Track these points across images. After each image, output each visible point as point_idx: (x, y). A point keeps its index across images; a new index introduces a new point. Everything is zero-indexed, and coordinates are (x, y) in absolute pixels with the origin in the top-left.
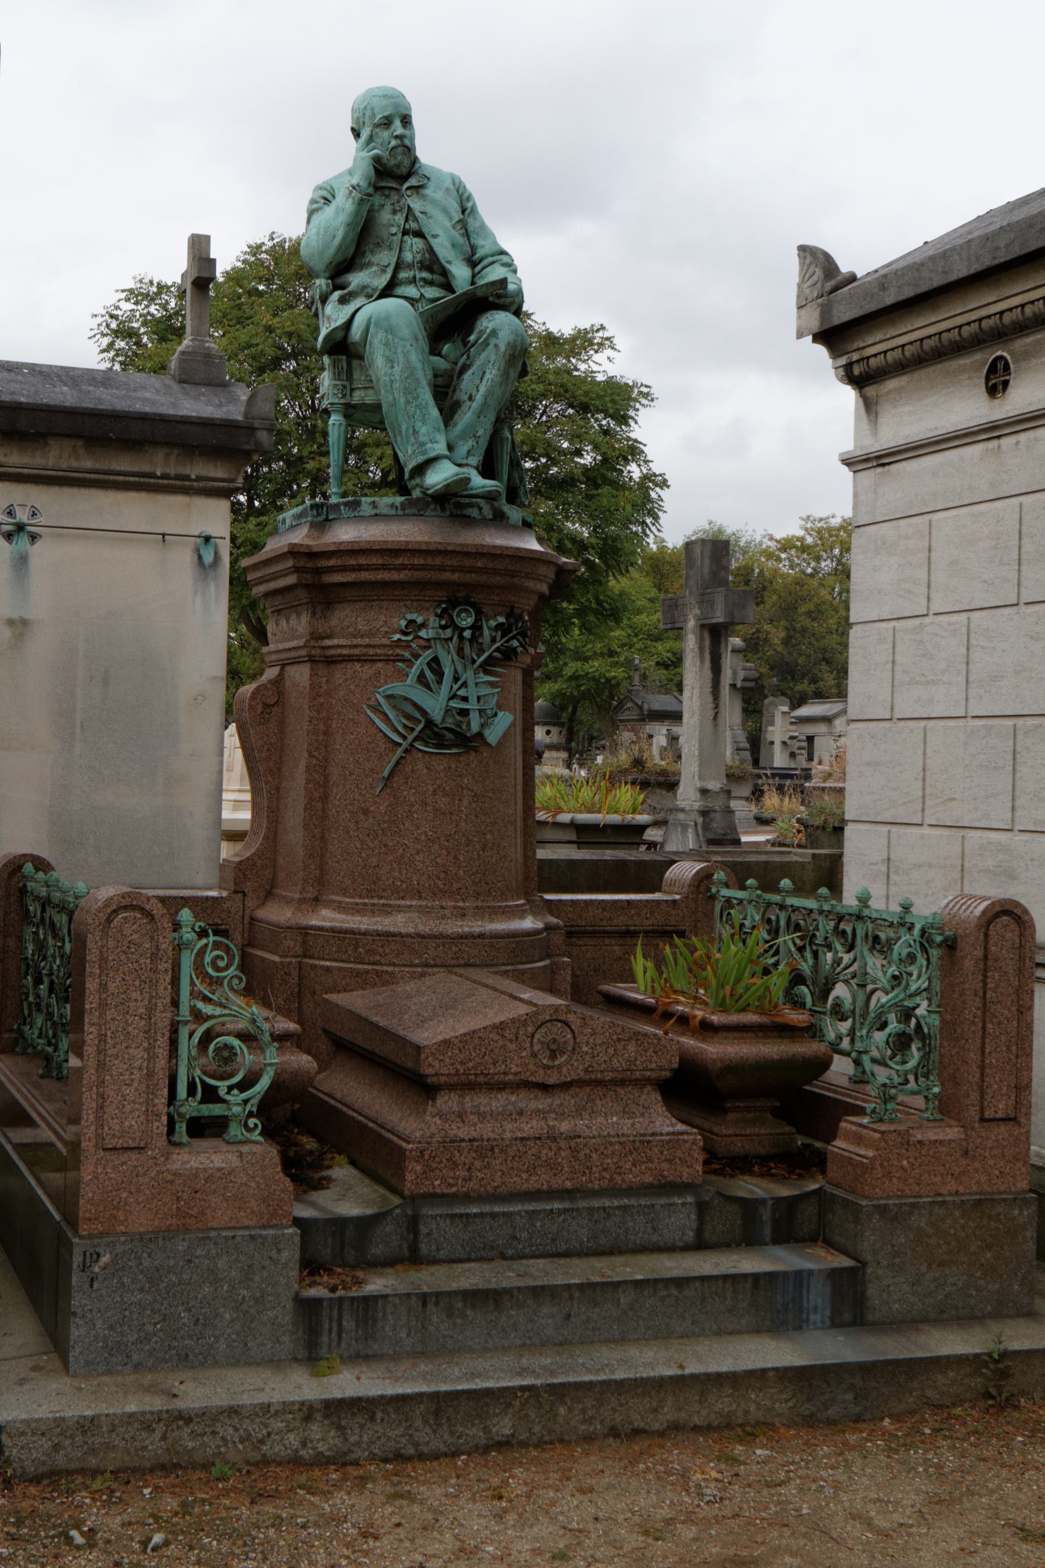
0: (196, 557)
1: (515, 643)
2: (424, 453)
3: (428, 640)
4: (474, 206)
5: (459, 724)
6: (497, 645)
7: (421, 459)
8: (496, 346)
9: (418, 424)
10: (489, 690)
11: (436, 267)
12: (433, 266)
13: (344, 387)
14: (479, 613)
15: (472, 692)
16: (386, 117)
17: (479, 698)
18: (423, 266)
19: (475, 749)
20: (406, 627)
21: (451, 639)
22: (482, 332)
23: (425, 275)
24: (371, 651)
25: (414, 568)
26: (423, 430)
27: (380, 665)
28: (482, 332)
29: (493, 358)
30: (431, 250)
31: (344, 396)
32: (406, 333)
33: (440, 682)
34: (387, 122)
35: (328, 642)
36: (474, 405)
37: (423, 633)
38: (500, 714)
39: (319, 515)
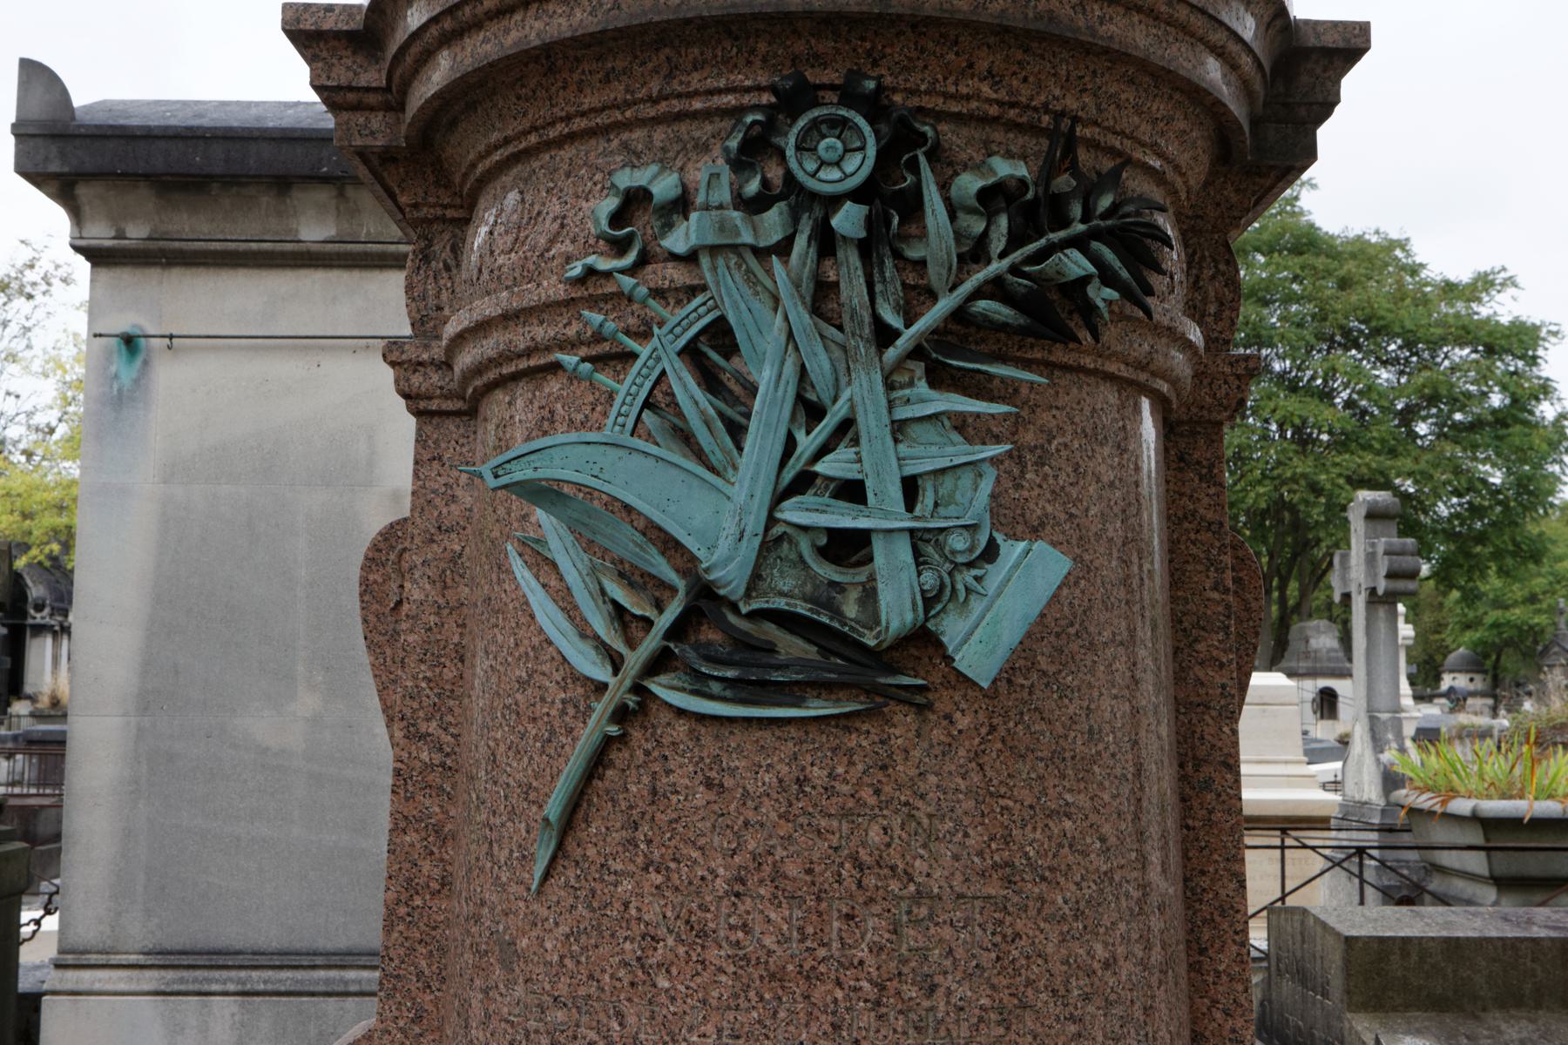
1: (1075, 264)
5: (827, 597)
6: (996, 267)
10: (959, 451)
15: (877, 462)
17: (911, 488)
19: (918, 701)
20: (617, 219)
21: (783, 248)
33: (736, 431)
37: (678, 240)
38: (1012, 551)
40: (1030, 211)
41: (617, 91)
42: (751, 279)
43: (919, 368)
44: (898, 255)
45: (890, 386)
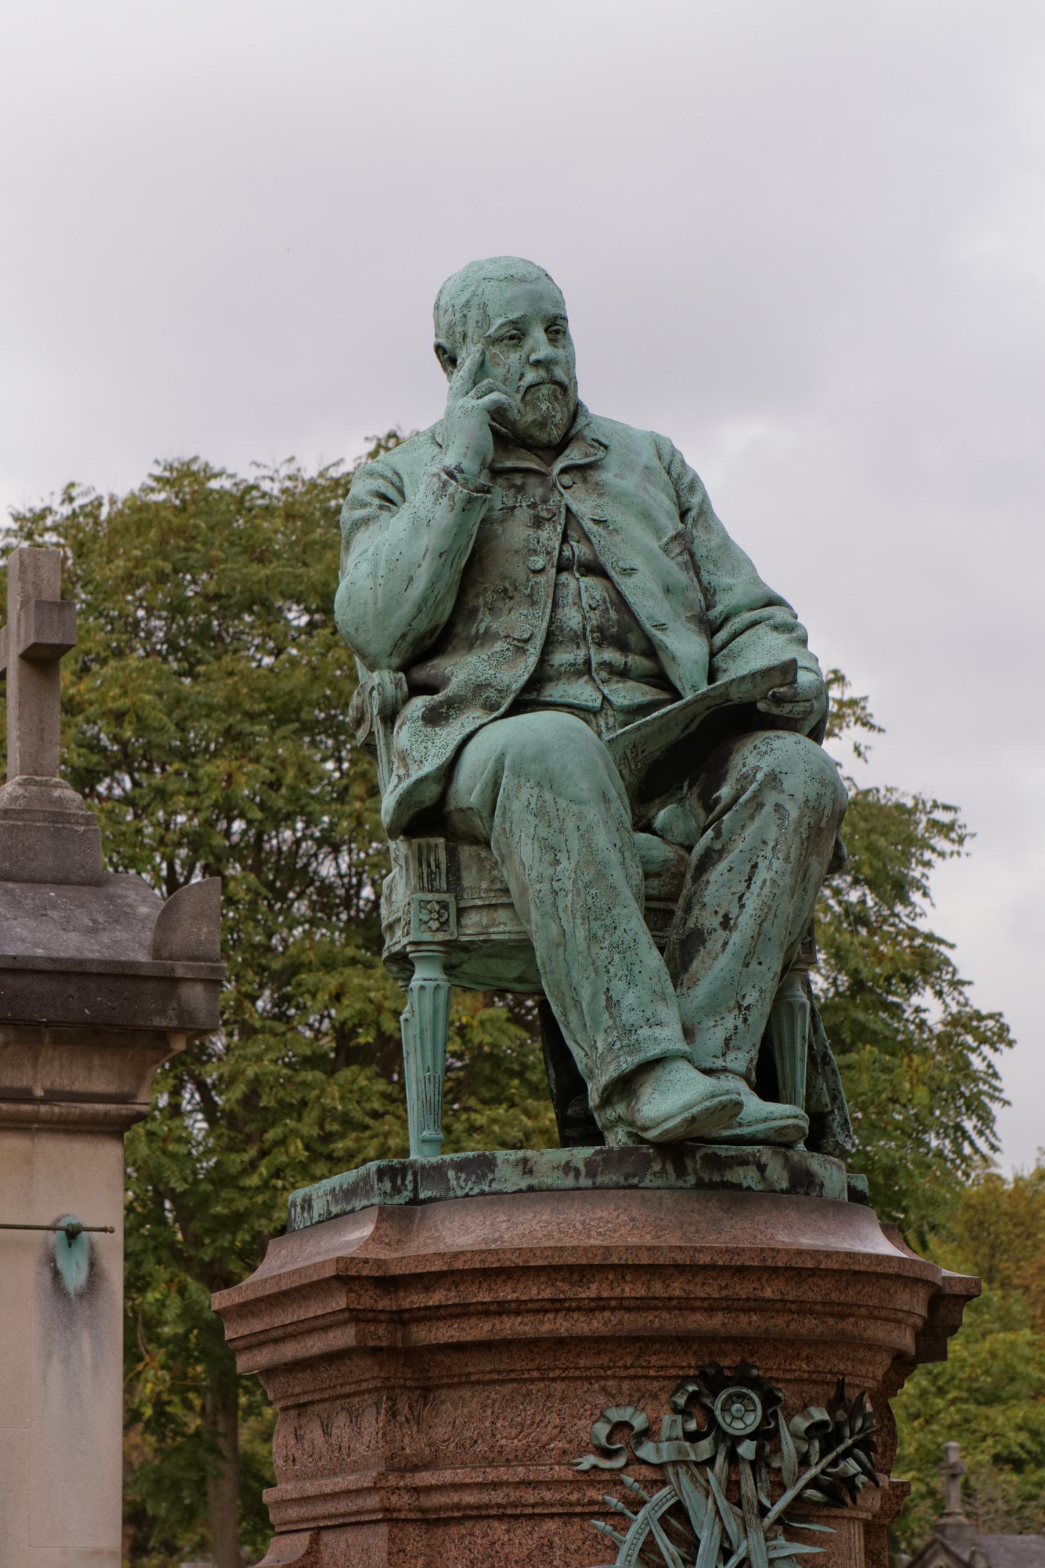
0: (48, 1275)
2: (634, 1048)
3: (661, 1467)
4: (705, 501)
6: (813, 1471)
7: (628, 1063)
8: (778, 807)
9: (618, 986)
11: (632, 638)
12: (625, 633)
13: (444, 906)
14: (770, 1400)
16: (514, 323)
18: (605, 638)
20: (609, 1437)
21: (711, 1462)
22: (746, 779)
23: (610, 655)
24: (531, 1496)
25: (623, 1305)
26: (630, 999)
27: (551, 1525)
28: (746, 779)
29: (772, 835)
30: (621, 602)
31: (444, 925)
32: (583, 787)
34: (515, 334)
35: (425, 1478)
36: (736, 937)
37: (647, 1451)
39: (396, 1190)
40: (826, 1436)
41: (604, 1360)
42: (693, 1479)
43: (780, 1529)
44: (768, 1465)
45: (766, 1540)
